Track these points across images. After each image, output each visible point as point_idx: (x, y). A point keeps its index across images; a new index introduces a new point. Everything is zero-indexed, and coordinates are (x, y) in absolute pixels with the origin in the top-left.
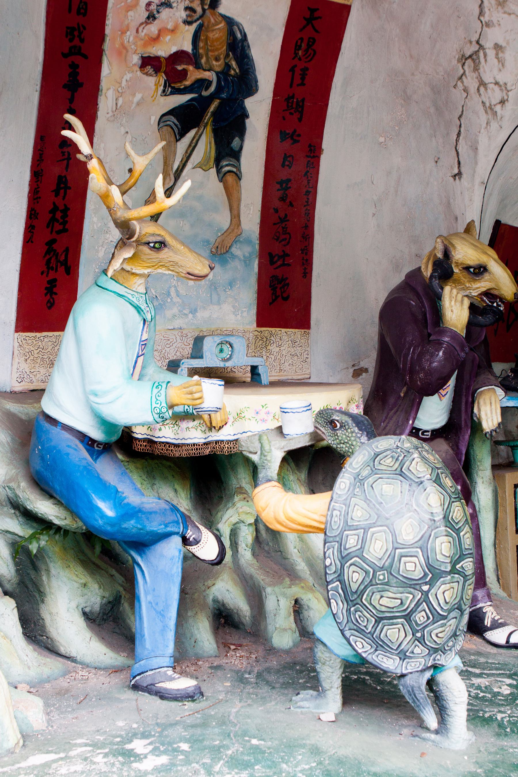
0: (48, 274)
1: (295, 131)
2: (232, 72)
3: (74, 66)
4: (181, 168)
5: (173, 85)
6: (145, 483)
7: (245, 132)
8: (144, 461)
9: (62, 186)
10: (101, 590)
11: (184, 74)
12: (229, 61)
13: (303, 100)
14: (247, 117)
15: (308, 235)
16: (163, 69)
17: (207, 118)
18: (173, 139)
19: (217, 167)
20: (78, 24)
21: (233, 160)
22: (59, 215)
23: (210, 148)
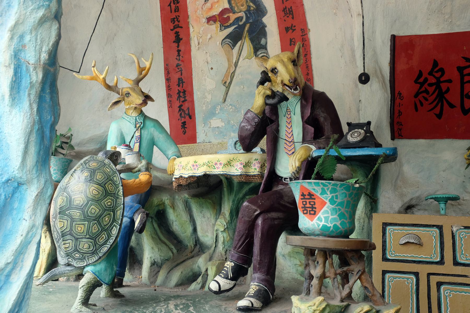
0: (181, 120)
1: (292, 25)
2: (252, 8)
3: (177, 33)
4: (237, 61)
5: (224, 25)
6: (198, 209)
7: (267, 34)
8: (198, 199)
9: (181, 82)
10: (159, 252)
11: (228, 18)
12: (249, 4)
13: (291, 7)
14: (266, 26)
15: (310, 78)
16: (218, 20)
17: (245, 34)
18: (230, 49)
19: (256, 56)
20: (176, 16)
21: (264, 50)
22: (181, 94)
23: (250, 47)
